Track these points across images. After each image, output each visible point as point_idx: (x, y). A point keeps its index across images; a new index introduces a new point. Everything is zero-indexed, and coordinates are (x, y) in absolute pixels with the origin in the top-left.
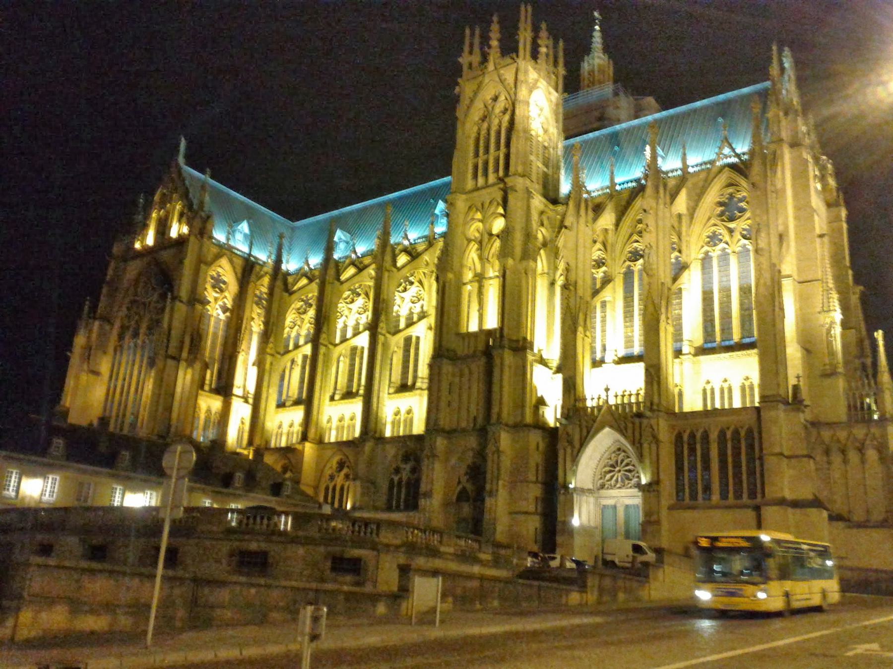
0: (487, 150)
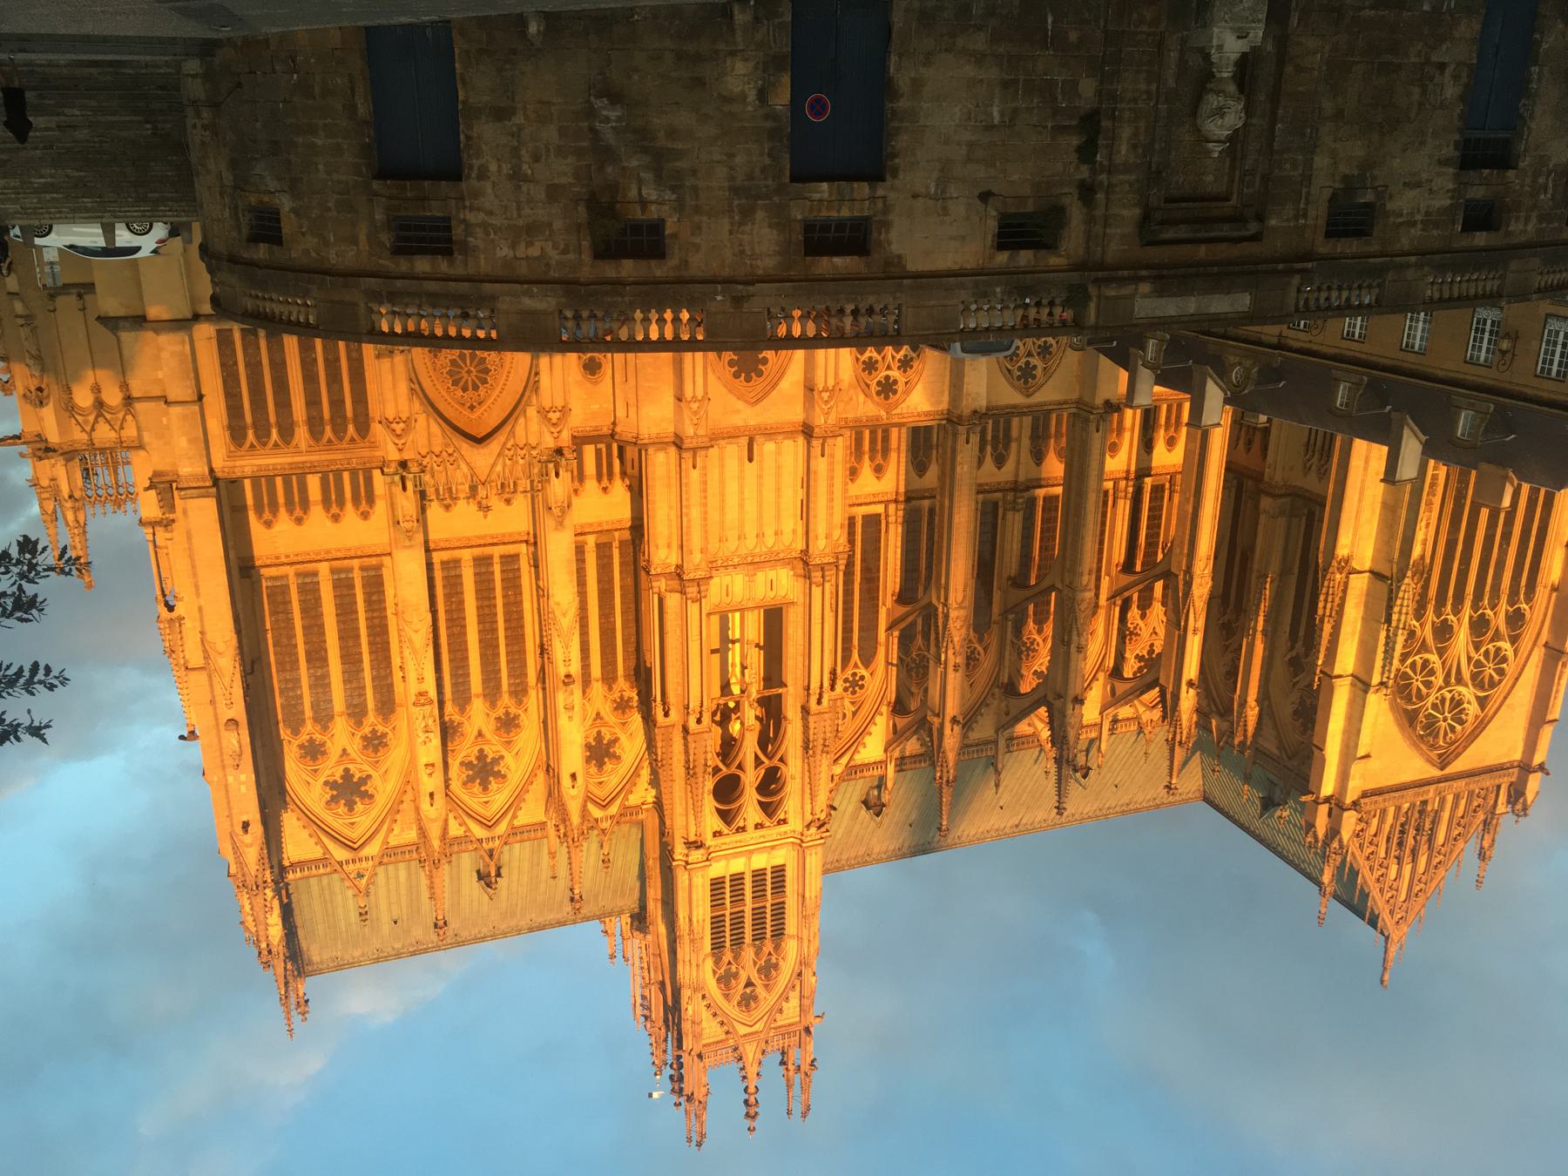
0: (759, 915)
